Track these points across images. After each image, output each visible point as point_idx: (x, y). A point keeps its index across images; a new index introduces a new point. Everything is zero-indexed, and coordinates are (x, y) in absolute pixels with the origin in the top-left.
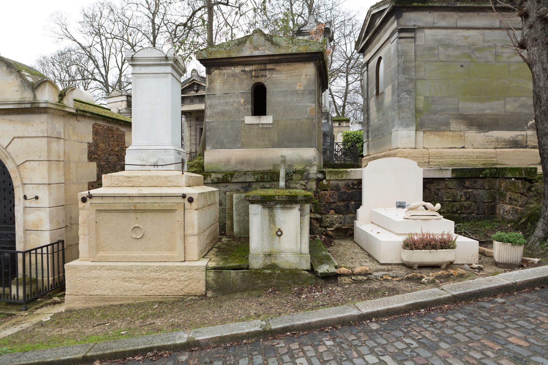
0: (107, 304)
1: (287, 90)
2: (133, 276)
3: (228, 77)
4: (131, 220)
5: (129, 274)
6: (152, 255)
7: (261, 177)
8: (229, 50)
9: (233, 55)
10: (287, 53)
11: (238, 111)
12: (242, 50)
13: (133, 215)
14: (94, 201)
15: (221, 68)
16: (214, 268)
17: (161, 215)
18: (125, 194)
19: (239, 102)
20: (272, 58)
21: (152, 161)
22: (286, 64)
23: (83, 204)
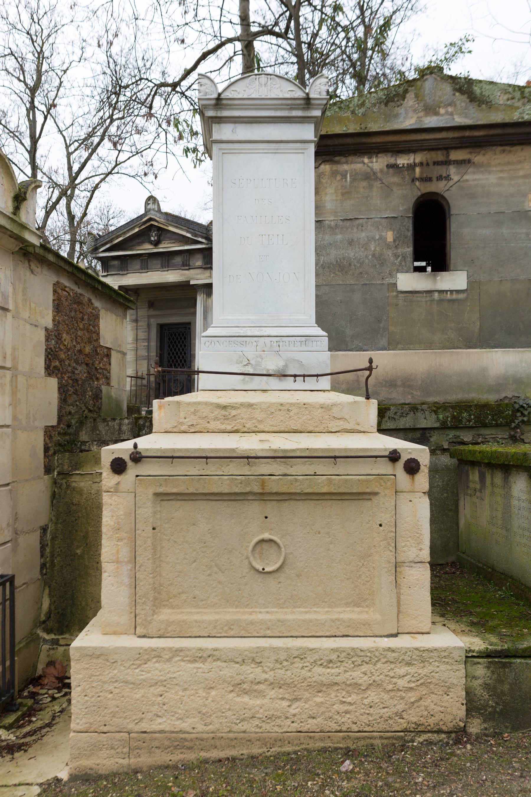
0: (191, 756)
1: (502, 209)
2: (264, 676)
3: (353, 180)
4: (251, 523)
5: (252, 672)
6: (308, 617)
7: (454, 417)
8: (364, 115)
9: (374, 127)
10: (507, 120)
11: (380, 260)
12: (397, 116)
13: (254, 509)
14: (147, 469)
15: (337, 158)
16: (487, 655)
17: (332, 511)
18: (233, 450)
19: (382, 239)
20: (467, 133)
21: (272, 364)
22: (500, 148)
23: (116, 478)
